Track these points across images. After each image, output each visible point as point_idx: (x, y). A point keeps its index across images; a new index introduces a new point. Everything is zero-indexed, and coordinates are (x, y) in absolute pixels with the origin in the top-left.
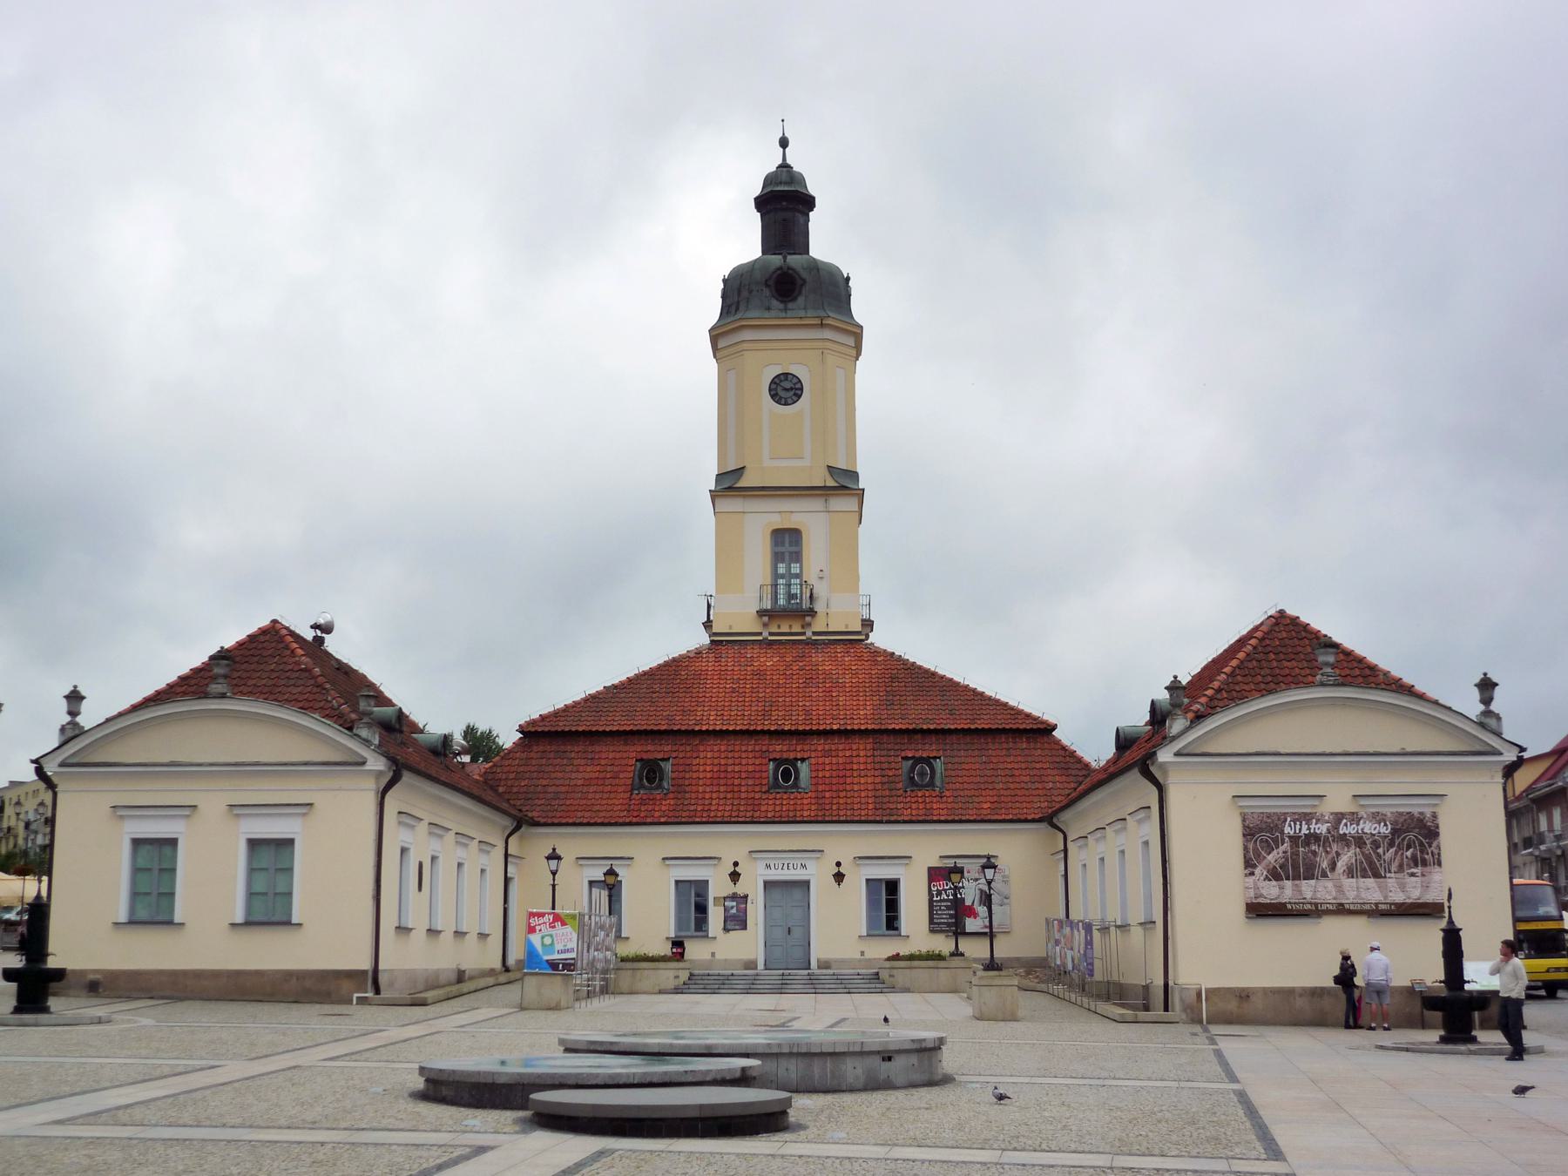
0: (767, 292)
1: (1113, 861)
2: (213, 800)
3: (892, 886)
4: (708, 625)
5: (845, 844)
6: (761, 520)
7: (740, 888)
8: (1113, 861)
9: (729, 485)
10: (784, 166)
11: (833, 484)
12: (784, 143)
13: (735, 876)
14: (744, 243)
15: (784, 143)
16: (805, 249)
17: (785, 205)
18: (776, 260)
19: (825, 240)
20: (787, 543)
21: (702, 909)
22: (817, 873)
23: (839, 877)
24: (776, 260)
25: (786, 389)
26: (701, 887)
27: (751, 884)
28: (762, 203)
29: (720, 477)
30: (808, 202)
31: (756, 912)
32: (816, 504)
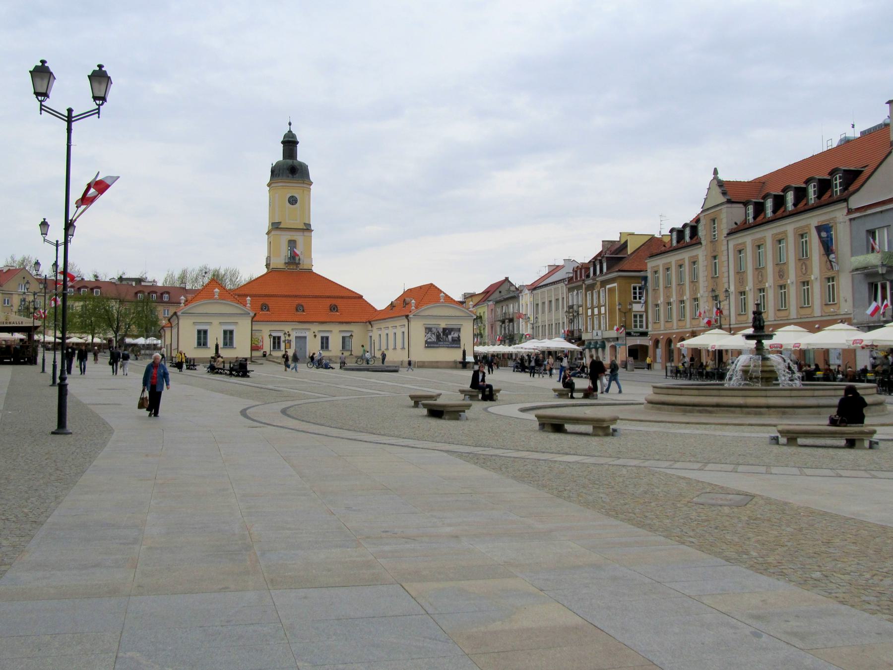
1: (391, 337)
2: (216, 321)
3: (327, 338)
4: (268, 266)
5: (315, 328)
6: (285, 237)
7: (290, 338)
8: (391, 337)
9: (275, 226)
10: (290, 131)
12: (290, 124)
14: (277, 155)
15: (290, 124)
17: (290, 144)
19: (302, 156)
20: (292, 243)
21: (279, 343)
22: (309, 335)
23: (315, 336)
24: (290, 161)
25: (293, 201)
26: (279, 338)
27: (293, 338)
28: (283, 142)
29: (273, 224)
30: (297, 143)
31: (293, 344)
32: (301, 233)
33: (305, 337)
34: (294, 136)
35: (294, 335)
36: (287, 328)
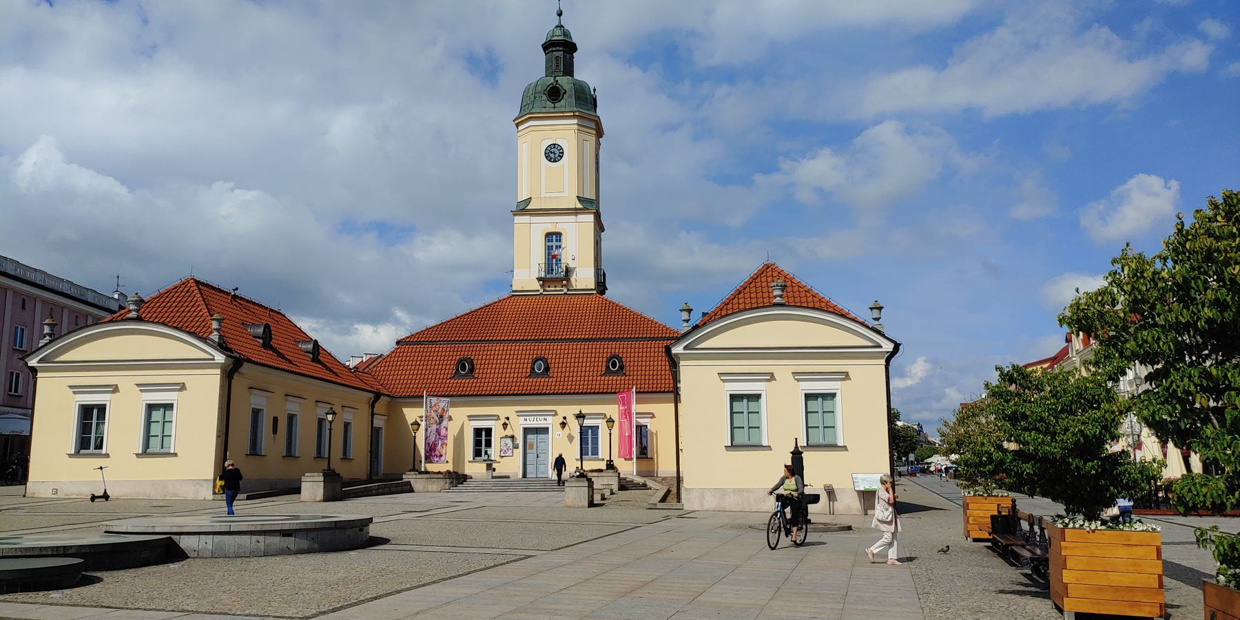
0: (544, 97)
2: (127, 381)
5: (568, 410)
11: (579, 206)
12: (560, 14)
13: (505, 425)
15: (560, 14)
16: (569, 71)
17: (561, 50)
18: (551, 80)
25: (554, 153)
26: (489, 431)
28: (546, 47)
32: (572, 218)
33: (545, 430)
34: (566, 34)
35: (518, 425)
36: (503, 411)
